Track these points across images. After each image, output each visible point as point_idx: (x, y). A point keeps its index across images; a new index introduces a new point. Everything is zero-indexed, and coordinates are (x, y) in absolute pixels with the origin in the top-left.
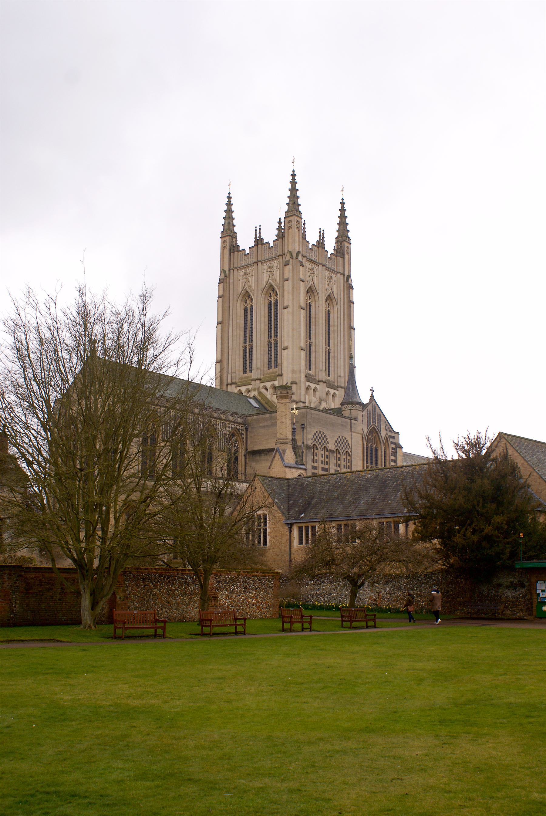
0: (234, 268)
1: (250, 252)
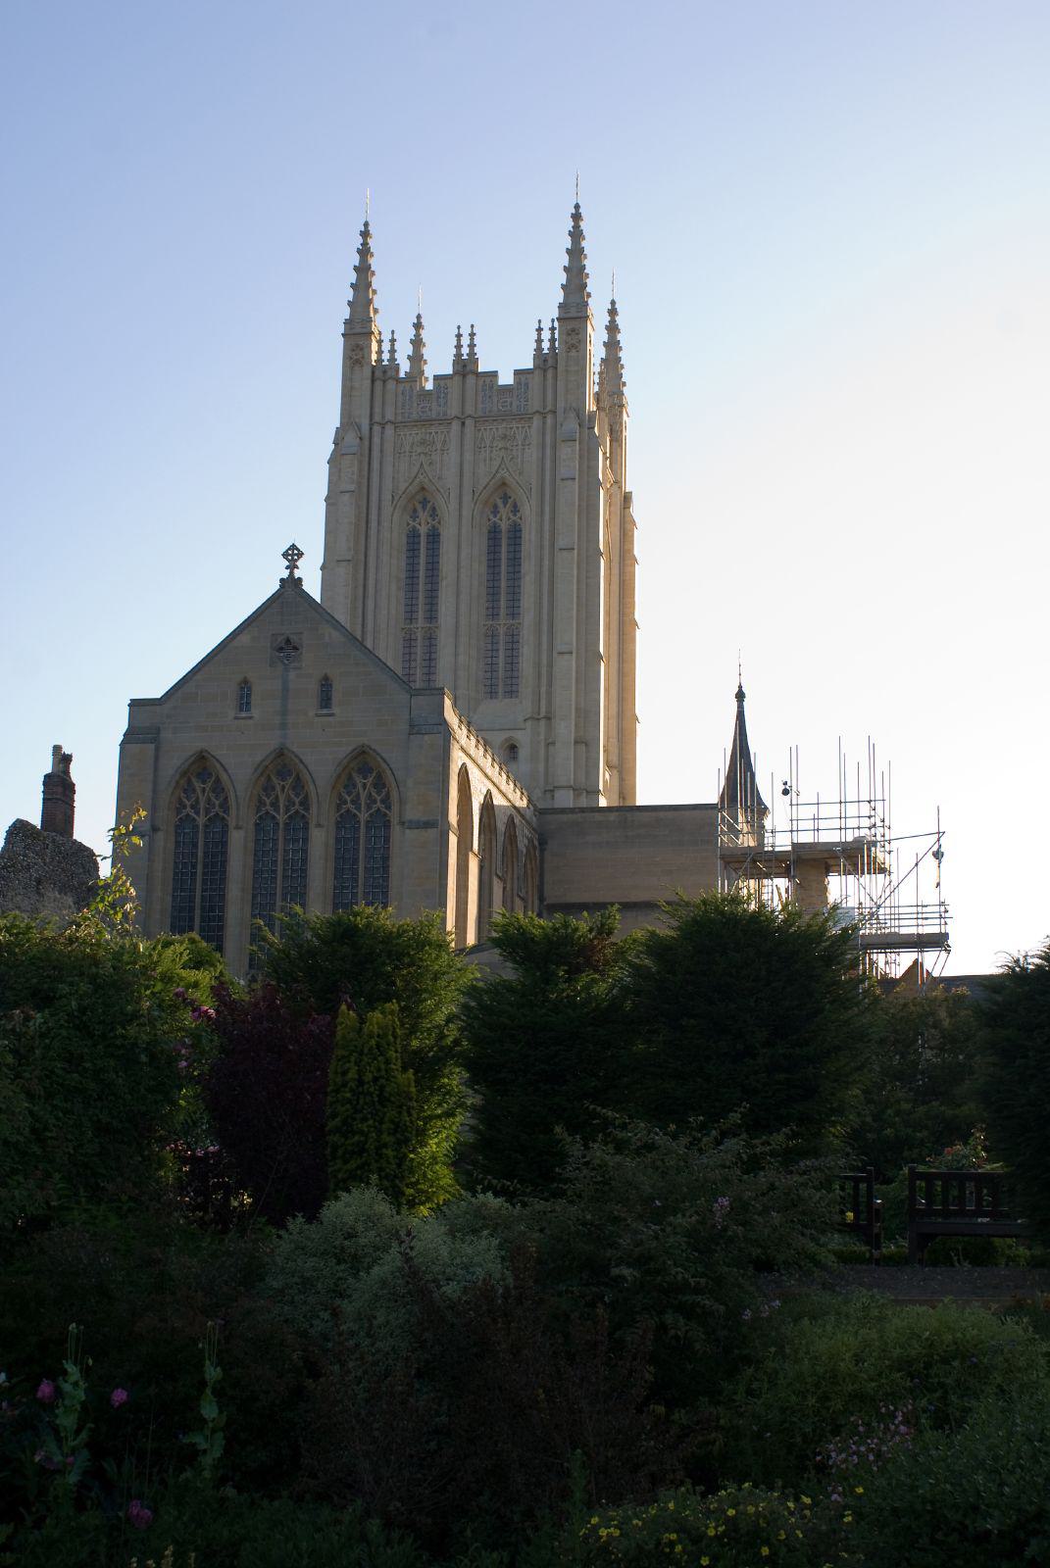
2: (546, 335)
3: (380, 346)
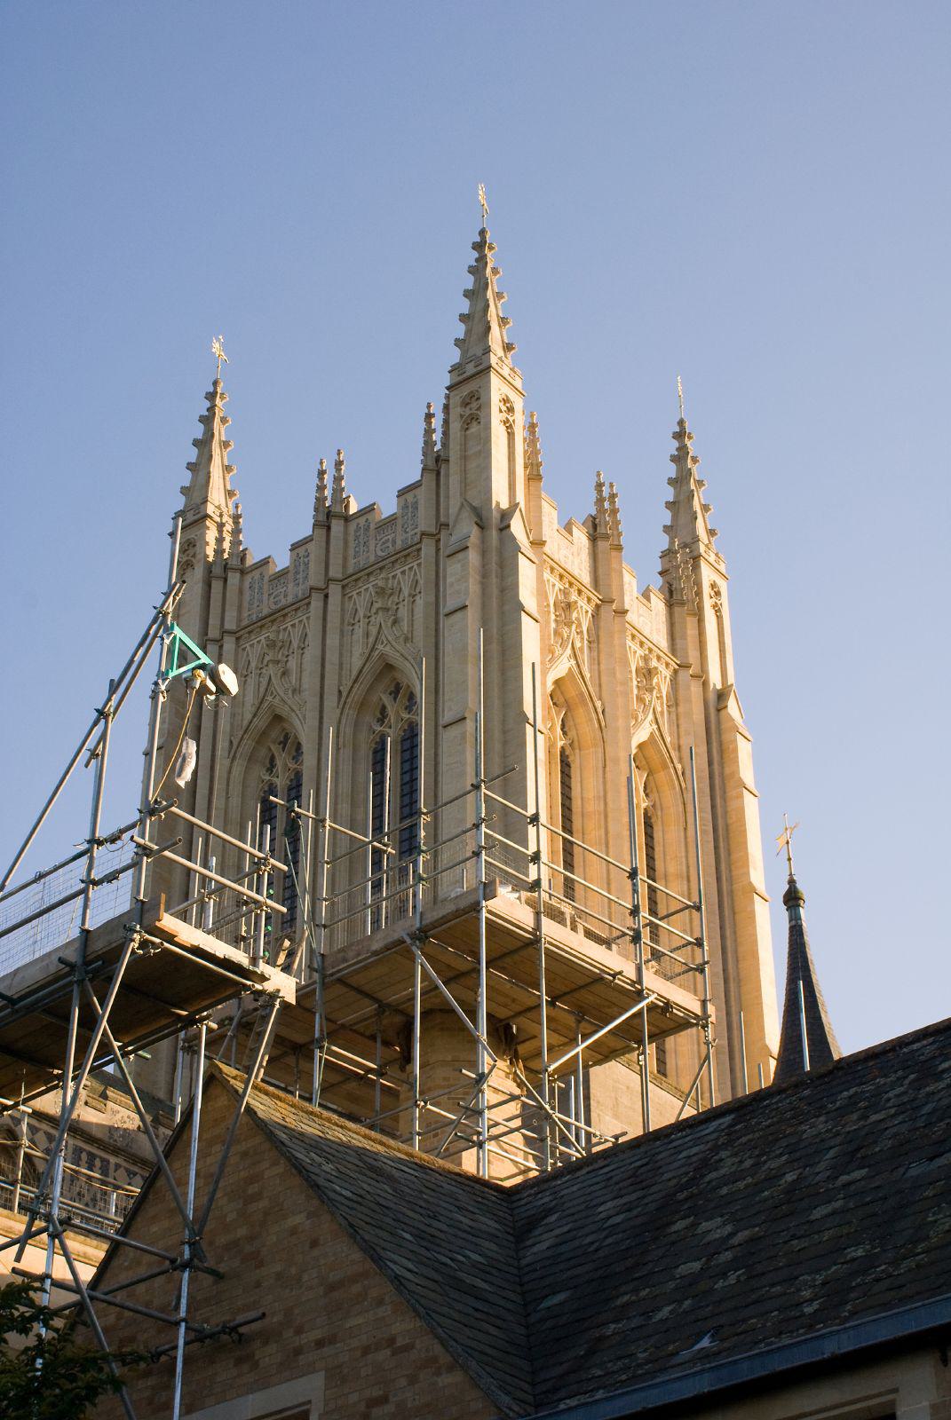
0: (224, 632)
1: (296, 561)
2: (437, 423)
3: (220, 531)
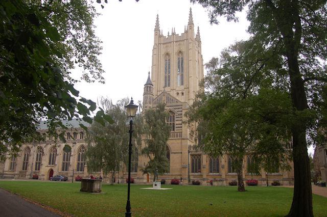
2: (186, 27)
